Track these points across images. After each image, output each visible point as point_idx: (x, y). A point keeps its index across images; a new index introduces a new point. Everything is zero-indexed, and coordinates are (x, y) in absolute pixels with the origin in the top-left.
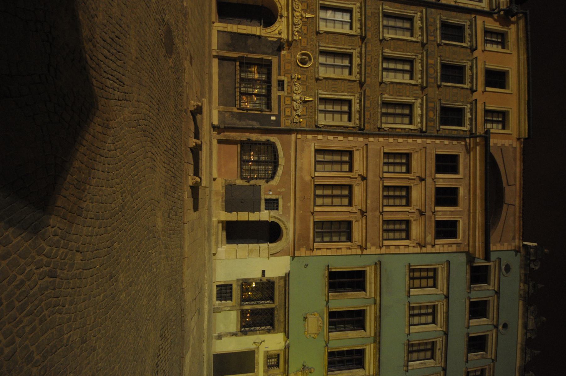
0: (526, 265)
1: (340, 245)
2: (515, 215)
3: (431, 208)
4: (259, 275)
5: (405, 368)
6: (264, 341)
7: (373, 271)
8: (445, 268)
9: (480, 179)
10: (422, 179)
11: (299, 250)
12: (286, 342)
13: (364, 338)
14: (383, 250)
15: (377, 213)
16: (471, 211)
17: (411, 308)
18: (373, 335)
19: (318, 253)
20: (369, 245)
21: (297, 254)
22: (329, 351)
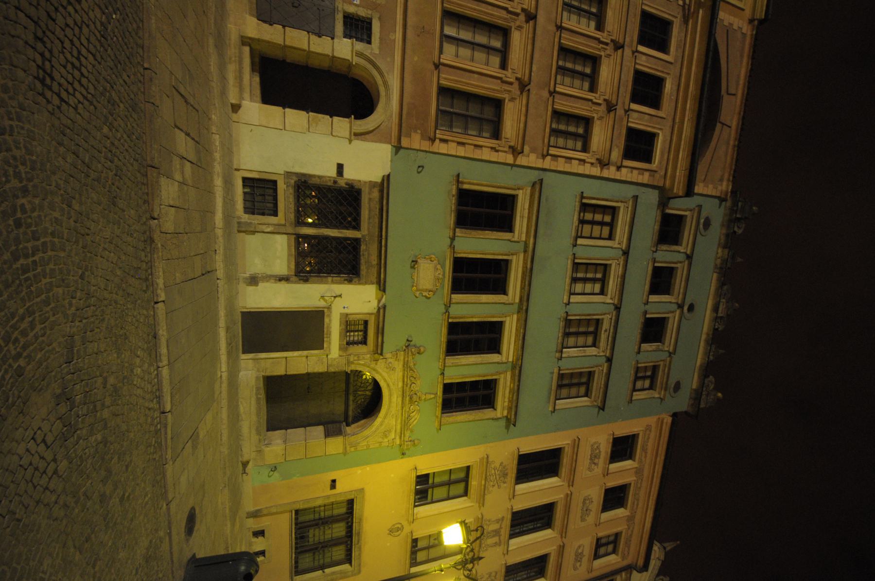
0: (731, 221)
1: (481, 141)
2: (728, 144)
3: (624, 103)
4: (332, 172)
5: (558, 355)
6: (340, 296)
7: (528, 197)
8: (630, 208)
9: (697, 66)
10: (618, 46)
11: (409, 135)
12: (379, 301)
13: (504, 303)
14: (548, 163)
15: (545, 94)
16: (677, 120)
17: (576, 266)
18: (517, 300)
19: (443, 148)
20: (527, 149)
21: (405, 142)
22: (450, 320)
